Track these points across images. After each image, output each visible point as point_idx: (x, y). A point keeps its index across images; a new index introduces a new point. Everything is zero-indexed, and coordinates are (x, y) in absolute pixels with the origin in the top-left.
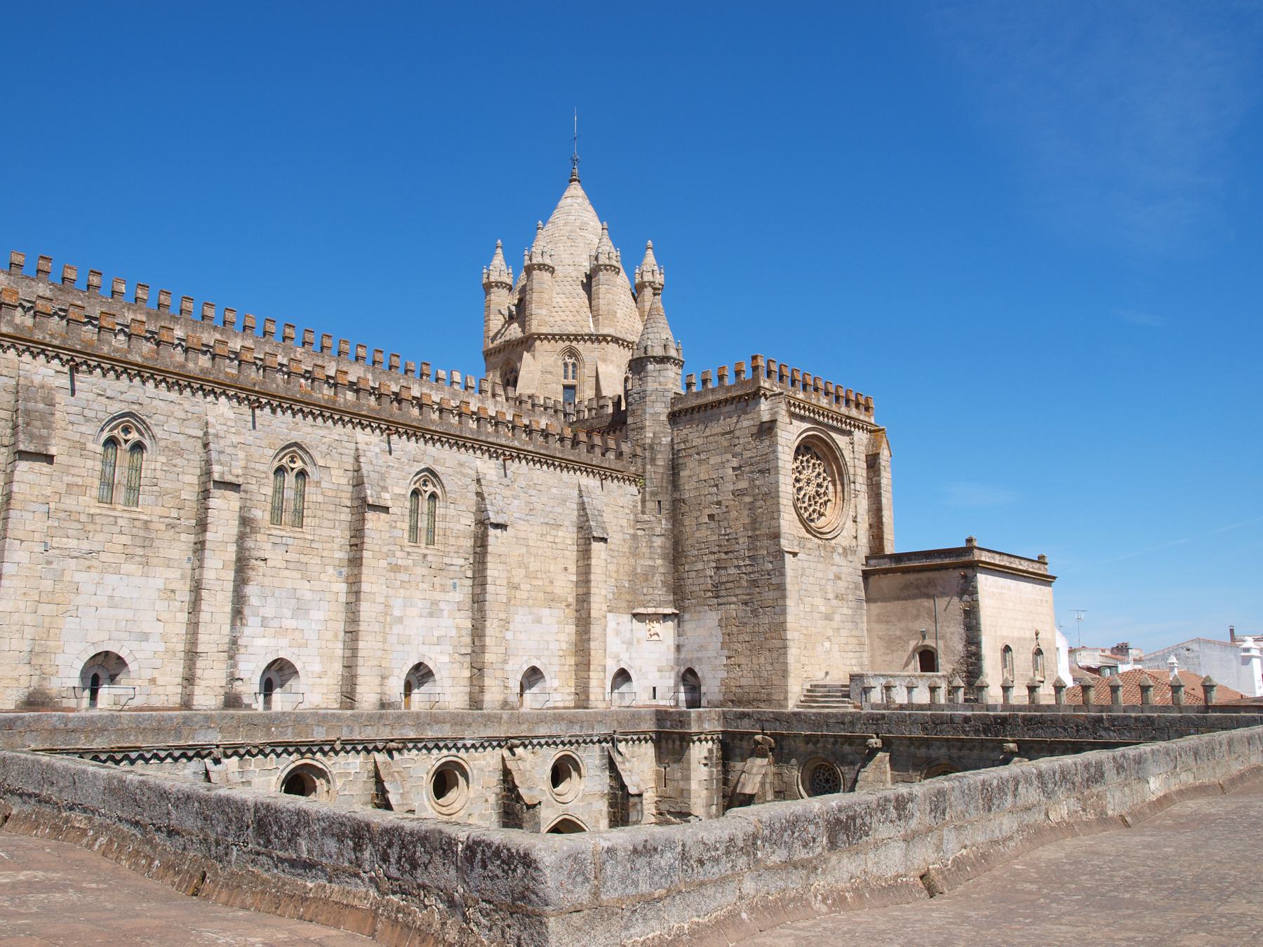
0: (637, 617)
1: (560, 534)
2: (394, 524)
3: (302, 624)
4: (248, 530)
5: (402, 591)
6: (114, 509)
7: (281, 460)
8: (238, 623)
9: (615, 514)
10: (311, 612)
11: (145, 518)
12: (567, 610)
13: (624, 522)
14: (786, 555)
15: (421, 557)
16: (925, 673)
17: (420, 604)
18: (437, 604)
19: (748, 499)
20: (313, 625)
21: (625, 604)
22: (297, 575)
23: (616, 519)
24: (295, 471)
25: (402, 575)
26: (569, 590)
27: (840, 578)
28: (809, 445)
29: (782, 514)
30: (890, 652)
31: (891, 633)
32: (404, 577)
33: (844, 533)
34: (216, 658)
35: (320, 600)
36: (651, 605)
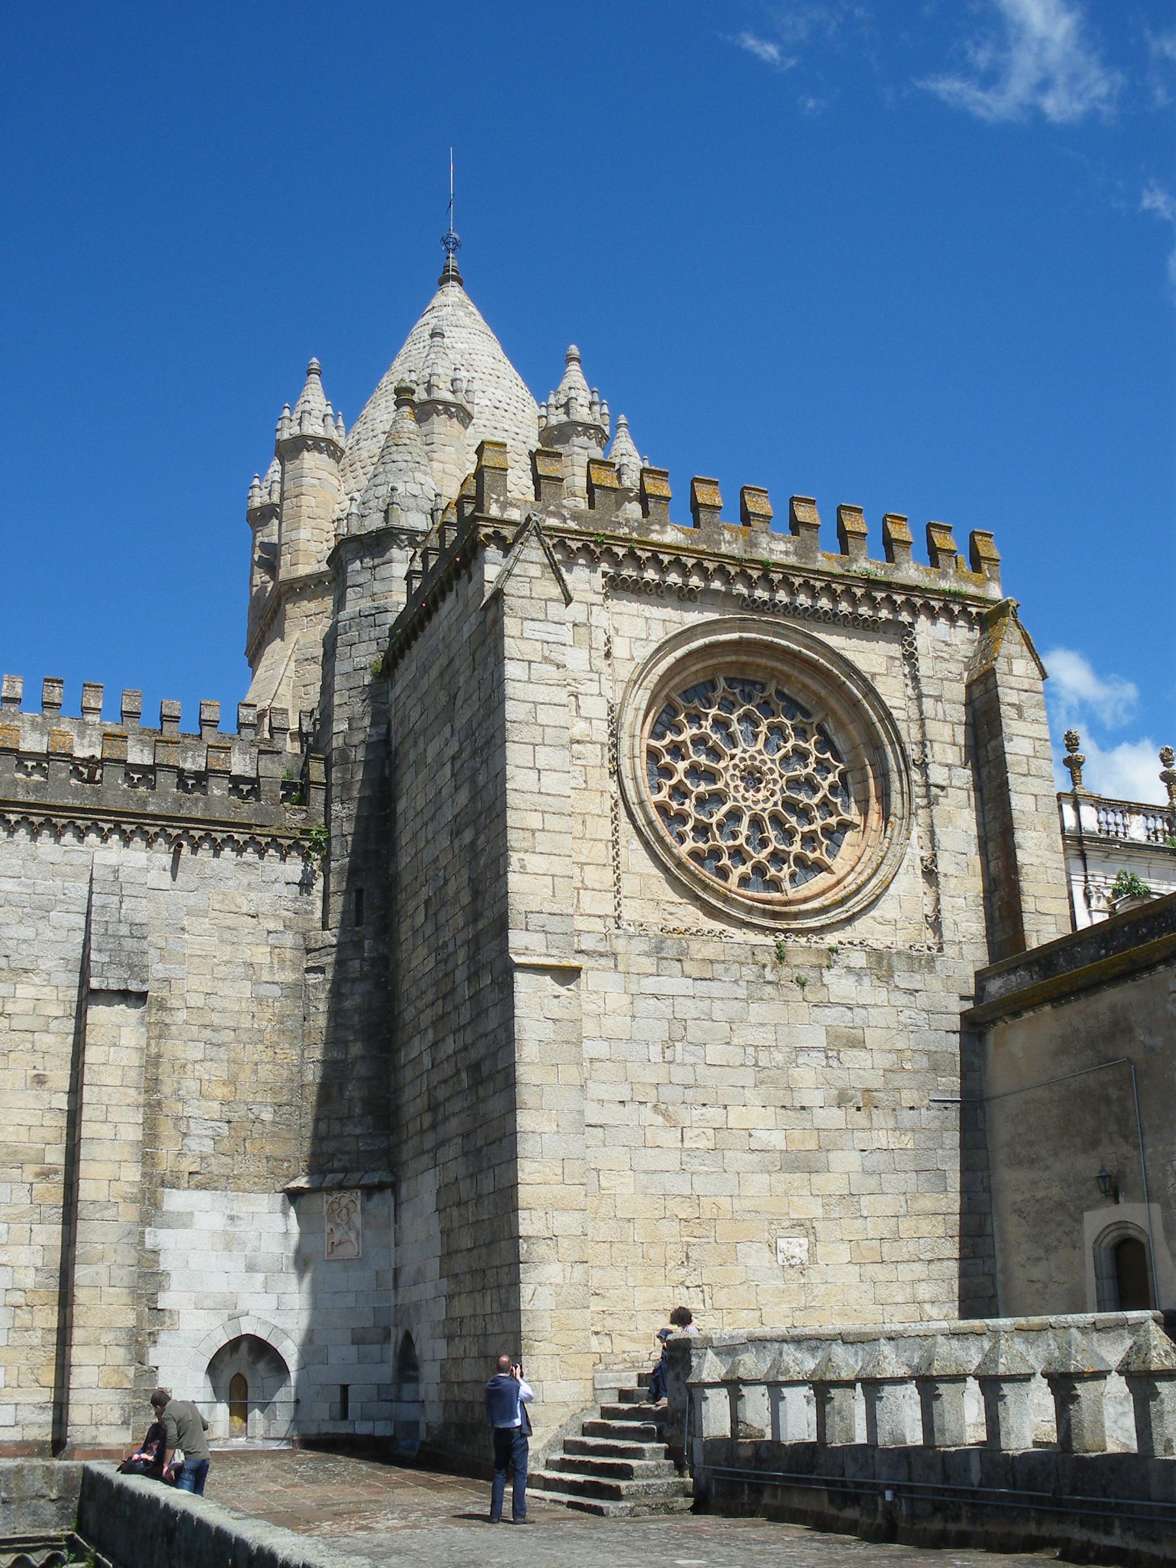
0: (303, 1201)
1: (23, 991)
9: (227, 935)
12: (40, 1187)
13: (261, 955)
14: (519, 976)
16: (976, 1323)
19: (468, 836)
21: (263, 1168)
23: (229, 948)
26: (51, 1135)
27: (858, 1043)
28: (759, 677)
29: (514, 858)
30: (1041, 1253)
31: (1040, 1194)
33: (886, 909)
36: (337, 1164)
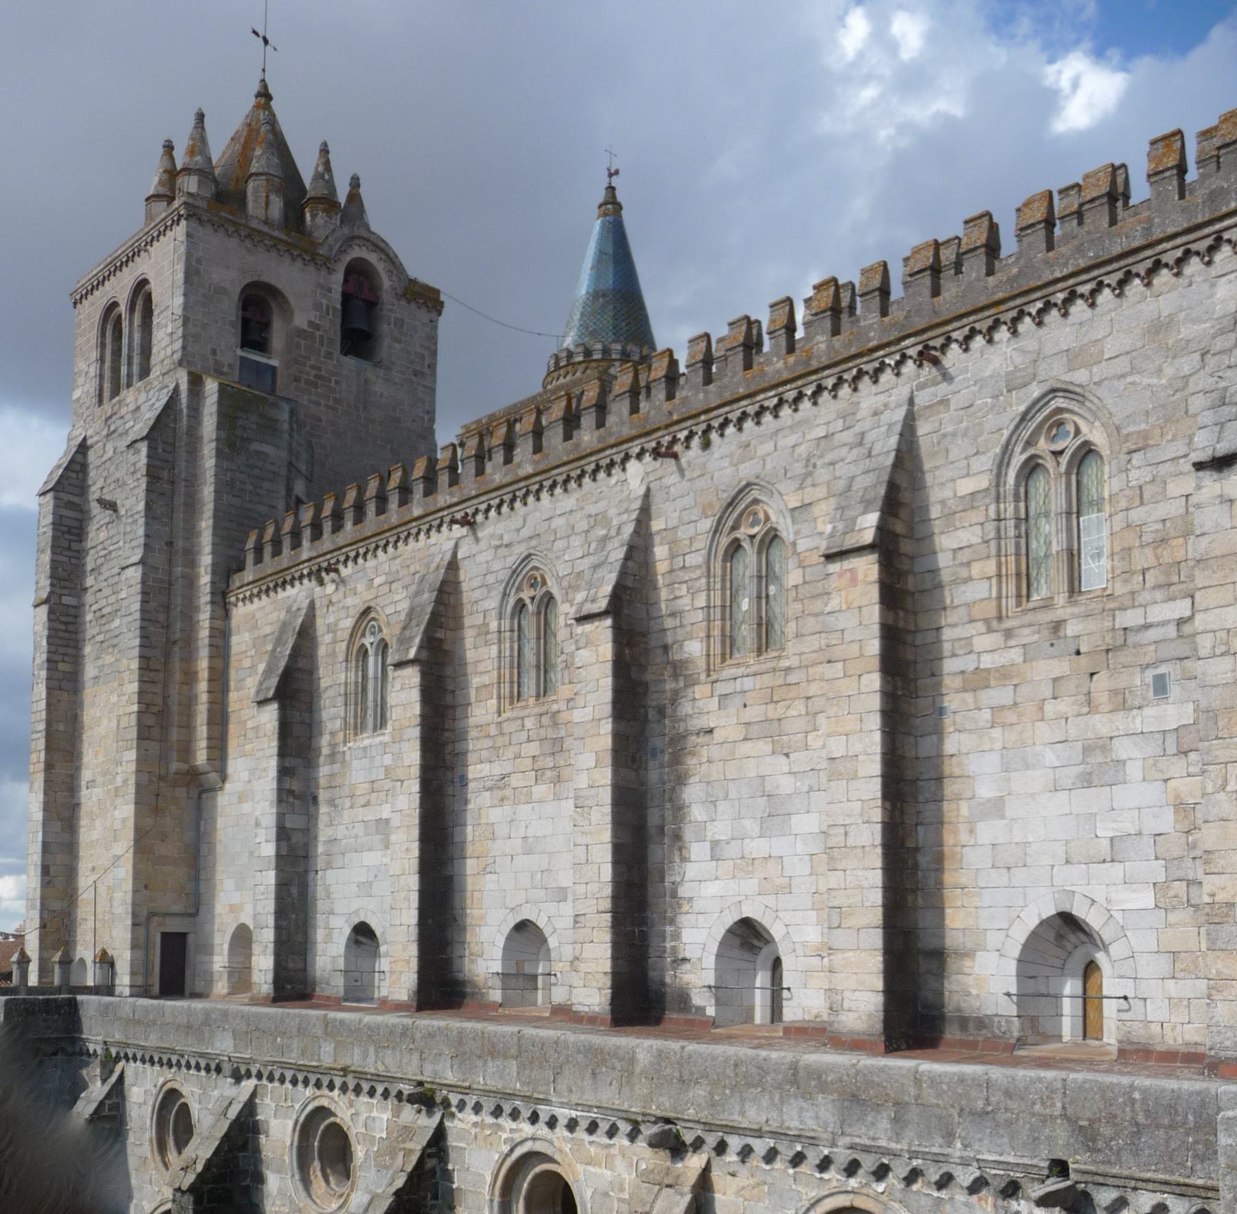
2: (964, 573)
3: (778, 846)
4: (681, 684)
5: (997, 733)
6: (526, 707)
7: (734, 528)
8: (677, 859)
10: (794, 819)
11: (555, 707)
15: (1046, 633)
17: (1050, 757)
18: (1105, 749)
20: (800, 848)
22: (764, 747)
24: (758, 538)
25: (991, 692)
32: (1000, 695)
34: (595, 924)
35: (811, 790)
